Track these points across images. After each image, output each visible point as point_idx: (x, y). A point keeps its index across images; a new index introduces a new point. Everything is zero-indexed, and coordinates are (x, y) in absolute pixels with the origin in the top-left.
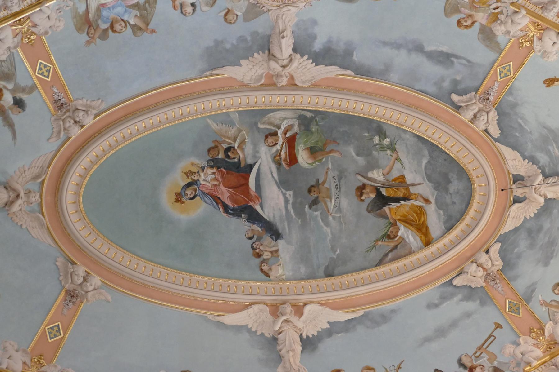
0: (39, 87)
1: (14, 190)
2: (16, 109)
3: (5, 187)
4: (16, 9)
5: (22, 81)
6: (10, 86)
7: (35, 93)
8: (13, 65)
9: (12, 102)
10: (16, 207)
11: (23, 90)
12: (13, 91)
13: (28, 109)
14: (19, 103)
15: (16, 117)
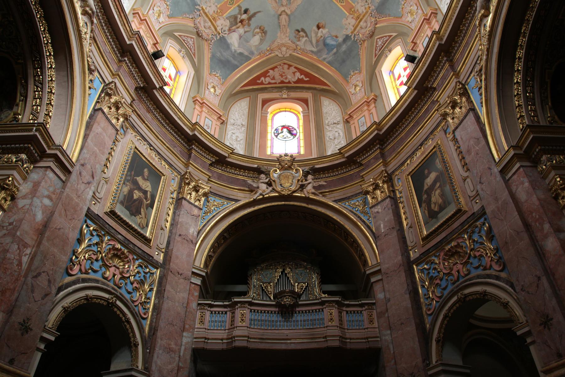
0: (238, 3)
1: (282, 12)
2: (248, 12)
3: (280, 15)
4: (210, 24)
5: (237, 11)
6: (239, 16)
7: (241, 5)
8: (230, 17)
9: (245, 15)
10: (289, 13)
11: (240, 10)
12: (241, 15)
13: (248, 7)
14: (246, 11)
15: (251, 12)
